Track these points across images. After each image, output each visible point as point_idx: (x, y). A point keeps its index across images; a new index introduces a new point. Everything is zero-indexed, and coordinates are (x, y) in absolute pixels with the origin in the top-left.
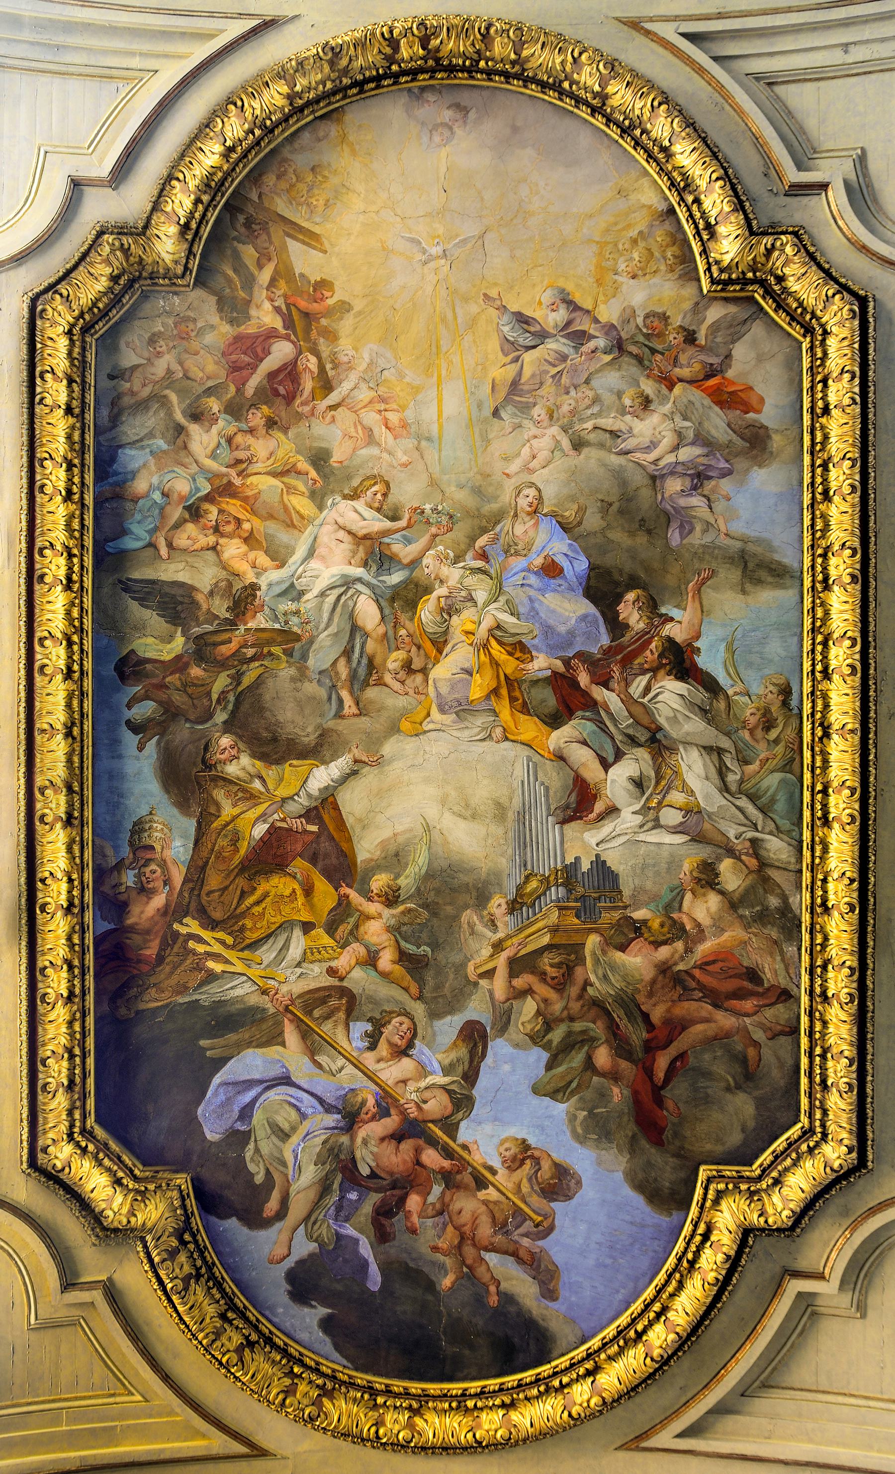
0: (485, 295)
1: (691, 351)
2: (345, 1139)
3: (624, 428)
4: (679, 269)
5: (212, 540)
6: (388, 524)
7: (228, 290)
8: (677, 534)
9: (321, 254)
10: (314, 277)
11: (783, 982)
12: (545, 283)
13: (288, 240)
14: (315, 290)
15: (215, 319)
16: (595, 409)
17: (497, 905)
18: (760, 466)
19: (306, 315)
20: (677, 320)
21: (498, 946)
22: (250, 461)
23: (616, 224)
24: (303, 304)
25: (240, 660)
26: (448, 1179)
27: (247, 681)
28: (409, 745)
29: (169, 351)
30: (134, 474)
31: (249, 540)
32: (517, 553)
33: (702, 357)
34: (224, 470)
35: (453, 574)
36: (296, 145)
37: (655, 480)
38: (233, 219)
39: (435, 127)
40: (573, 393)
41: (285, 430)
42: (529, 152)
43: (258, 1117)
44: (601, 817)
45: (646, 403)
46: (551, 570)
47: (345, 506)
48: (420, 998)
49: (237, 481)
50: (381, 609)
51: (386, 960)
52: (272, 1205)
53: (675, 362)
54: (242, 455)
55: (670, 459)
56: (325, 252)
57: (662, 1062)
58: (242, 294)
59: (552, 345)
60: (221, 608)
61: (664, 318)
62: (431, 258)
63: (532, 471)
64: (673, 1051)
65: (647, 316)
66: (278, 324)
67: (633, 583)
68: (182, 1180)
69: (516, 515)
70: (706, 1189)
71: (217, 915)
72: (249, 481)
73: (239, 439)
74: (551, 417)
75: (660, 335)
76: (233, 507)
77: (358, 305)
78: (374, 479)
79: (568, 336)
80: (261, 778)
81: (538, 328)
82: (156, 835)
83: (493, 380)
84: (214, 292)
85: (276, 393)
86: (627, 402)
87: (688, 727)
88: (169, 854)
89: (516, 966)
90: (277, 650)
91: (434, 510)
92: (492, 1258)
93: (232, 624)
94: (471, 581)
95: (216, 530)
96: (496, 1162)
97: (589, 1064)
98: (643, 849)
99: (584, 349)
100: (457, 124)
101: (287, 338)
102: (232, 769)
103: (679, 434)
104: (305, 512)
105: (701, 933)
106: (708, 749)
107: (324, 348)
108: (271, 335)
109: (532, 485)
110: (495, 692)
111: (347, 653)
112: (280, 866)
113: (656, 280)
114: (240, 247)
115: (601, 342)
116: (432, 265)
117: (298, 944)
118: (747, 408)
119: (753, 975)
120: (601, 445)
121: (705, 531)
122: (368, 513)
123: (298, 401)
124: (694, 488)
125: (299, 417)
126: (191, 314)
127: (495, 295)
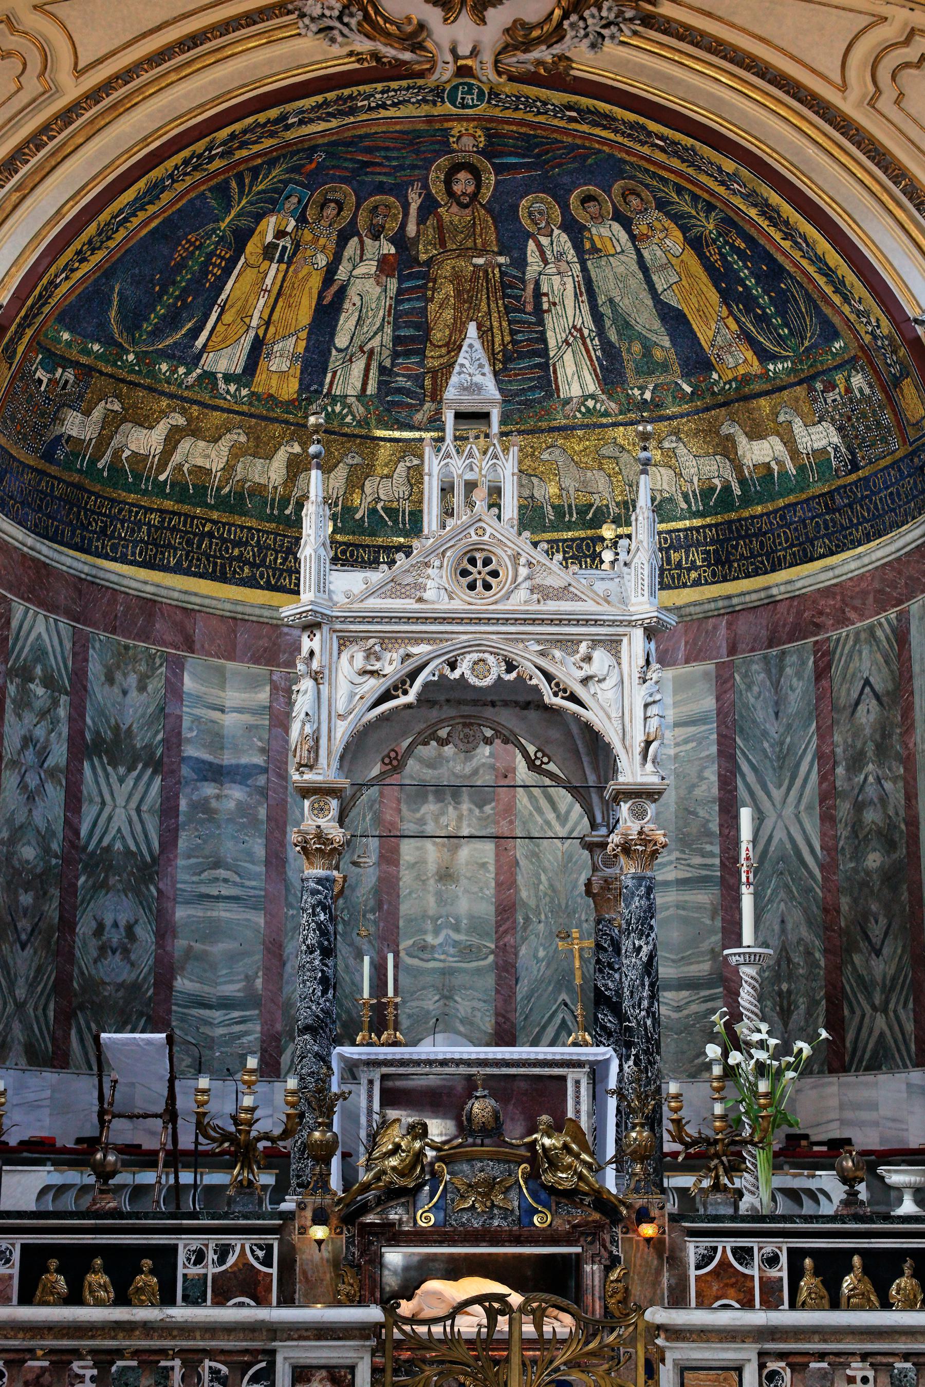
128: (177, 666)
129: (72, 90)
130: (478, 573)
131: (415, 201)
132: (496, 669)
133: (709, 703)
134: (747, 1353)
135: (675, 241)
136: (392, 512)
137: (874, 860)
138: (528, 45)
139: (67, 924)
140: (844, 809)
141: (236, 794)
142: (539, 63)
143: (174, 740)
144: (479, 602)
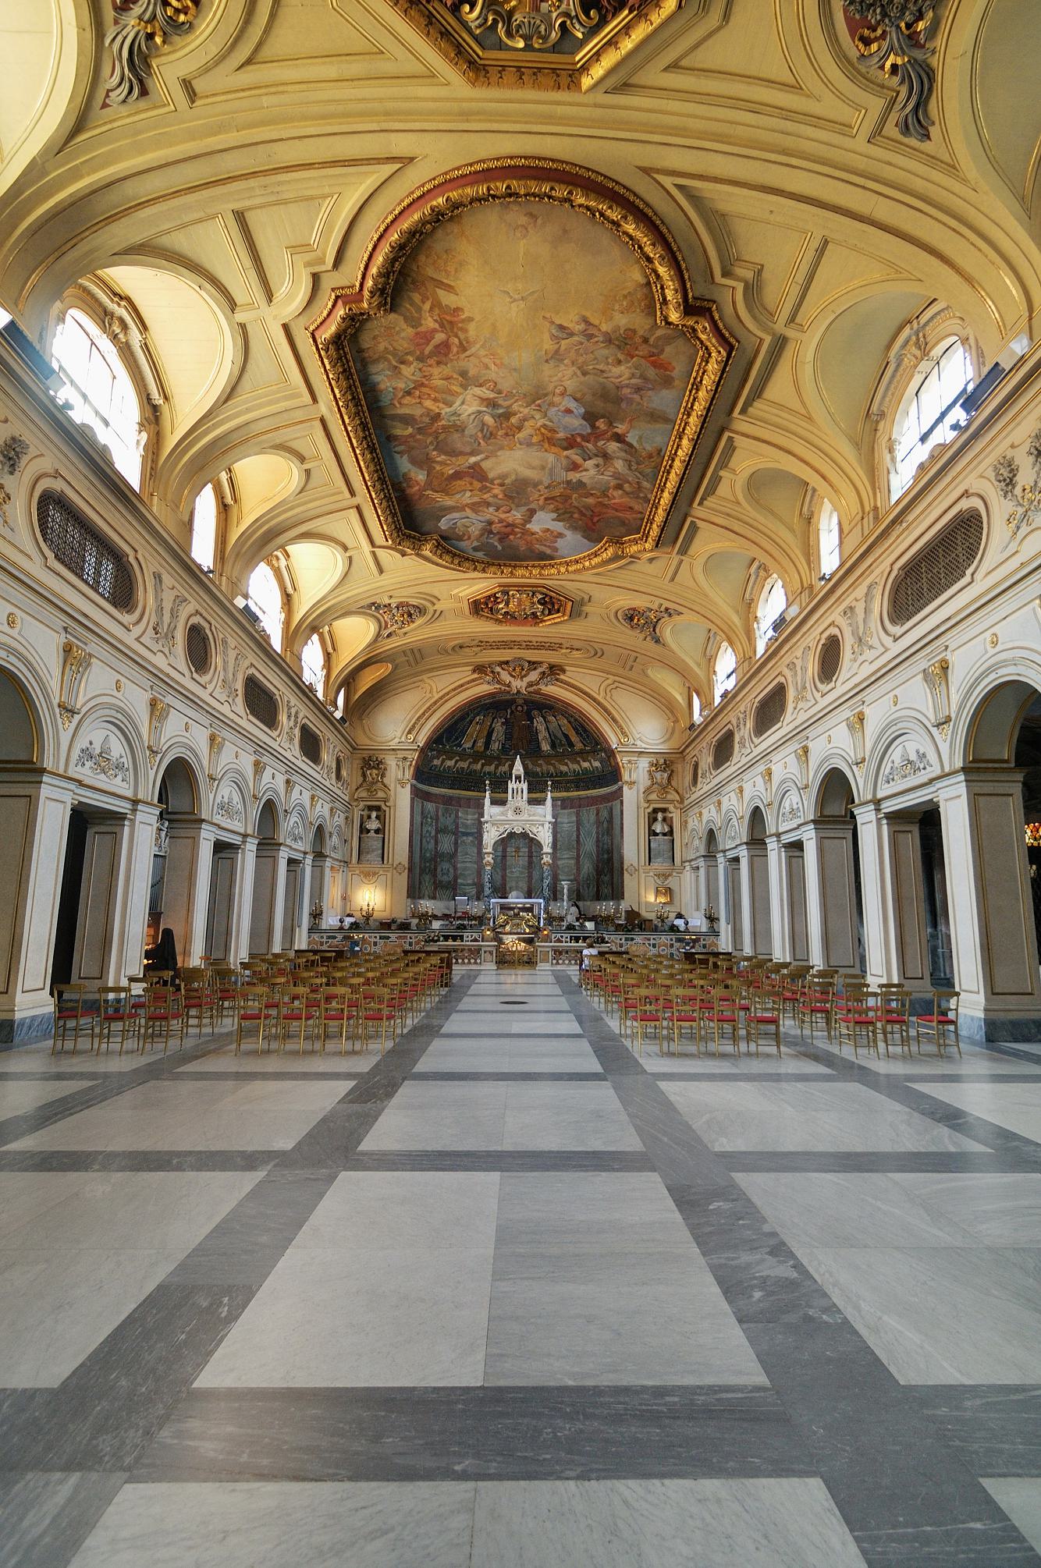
1: (644, 346)
4: (646, 311)
5: (418, 401)
10: (453, 306)
15: (405, 326)
16: (595, 362)
17: (539, 487)
19: (451, 323)
20: (641, 332)
22: (431, 375)
23: (617, 287)
24: (448, 318)
25: (436, 435)
26: (523, 533)
28: (508, 453)
30: (378, 383)
31: (435, 400)
35: (526, 411)
39: (517, 227)
41: (446, 365)
45: (619, 362)
46: (568, 411)
47: (476, 389)
49: (427, 382)
51: (500, 496)
52: (466, 537)
53: (637, 349)
54: (426, 374)
57: (596, 519)
59: (576, 338)
60: (427, 420)
61: (634, 331)
66: (437, 326)
67: (603, 417)
75: (631, 338)
76: (424, 390)
82: (413, 475)
86: (610, 360)
89: (546, 499)
93: (432, 424)
95: (419, 397)
97: (571, 516)
101: (442, 332)
102: (438, 459)
103: (633, 375)
105: (614, 498)
106: (626, 460)
107: (460, 334)
108: (434, 331)
111: (482, 430)
112: (461, 479)
113: (634, 315)
115: (601, 339)
117: (468, 494)
118: (666, 369)
120: (595, 374)
125: (452, 360)
128: (457, 813)
129: (437, 697)
130: (518, 811)
131: (509, 711)
132: (521, 830)
133: (575, 819)
134: (550, 949)
135: (565, 721)
136: (505, 773)
137: (606, 856)
138: (532, 686)
139: (436, 870)
140: (601, 844)
141: (471, 838)
143: (457, 827)
144: (518, 817)
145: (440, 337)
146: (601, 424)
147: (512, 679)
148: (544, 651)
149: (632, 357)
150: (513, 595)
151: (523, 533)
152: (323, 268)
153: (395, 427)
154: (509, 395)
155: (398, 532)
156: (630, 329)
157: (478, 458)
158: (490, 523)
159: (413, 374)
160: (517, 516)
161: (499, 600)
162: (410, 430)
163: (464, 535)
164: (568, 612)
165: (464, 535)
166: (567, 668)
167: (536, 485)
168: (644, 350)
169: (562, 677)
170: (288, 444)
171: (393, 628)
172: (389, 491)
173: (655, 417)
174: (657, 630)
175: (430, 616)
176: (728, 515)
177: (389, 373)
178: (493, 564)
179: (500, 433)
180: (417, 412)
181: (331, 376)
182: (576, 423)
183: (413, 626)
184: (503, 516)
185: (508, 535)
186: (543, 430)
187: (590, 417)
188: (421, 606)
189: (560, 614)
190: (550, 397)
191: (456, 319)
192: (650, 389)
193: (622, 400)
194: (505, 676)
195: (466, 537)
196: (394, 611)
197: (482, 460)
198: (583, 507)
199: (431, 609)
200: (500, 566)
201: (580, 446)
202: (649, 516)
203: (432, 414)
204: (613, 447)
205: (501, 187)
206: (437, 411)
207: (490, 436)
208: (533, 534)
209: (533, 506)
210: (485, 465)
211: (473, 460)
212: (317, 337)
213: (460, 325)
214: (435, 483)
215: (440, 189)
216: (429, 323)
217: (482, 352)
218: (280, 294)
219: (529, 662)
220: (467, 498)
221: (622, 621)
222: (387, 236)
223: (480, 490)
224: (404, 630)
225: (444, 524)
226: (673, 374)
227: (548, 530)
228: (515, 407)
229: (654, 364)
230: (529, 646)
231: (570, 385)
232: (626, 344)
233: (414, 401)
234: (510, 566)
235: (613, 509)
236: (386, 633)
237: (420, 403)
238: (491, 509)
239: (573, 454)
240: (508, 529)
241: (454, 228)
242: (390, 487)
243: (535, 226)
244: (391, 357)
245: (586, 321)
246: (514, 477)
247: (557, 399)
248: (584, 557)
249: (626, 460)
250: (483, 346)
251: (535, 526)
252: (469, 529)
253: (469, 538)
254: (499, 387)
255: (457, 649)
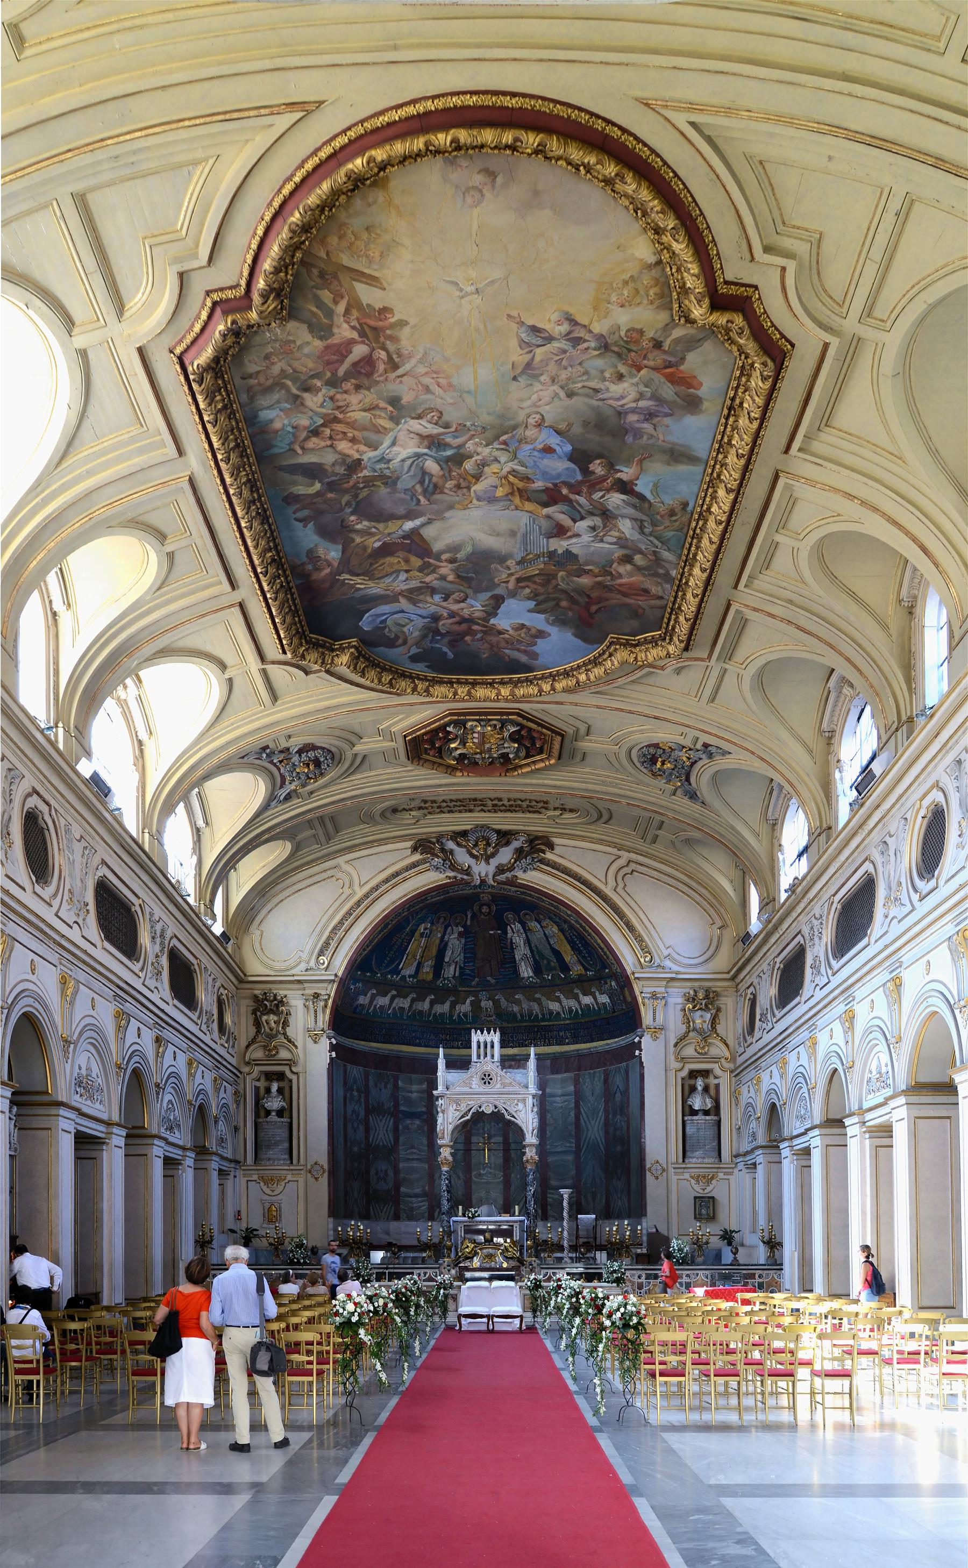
0: (509, 316)
1: (656, 353)
2: (433, 625)
3: (603, 387)
5: (329, 443)
6: (442, 430)
7: (314, 320)
8: (631, 439)
9: (381, 291)
11: (660, 594)
12: (555, 307)
13: (355, 283)
14: (379, 314)
15: (307, 337)
16: (585, 378)
17: (511, 563)
18: (692, 414)
19: (375, 329)
20: (650, 334)
21: (512, 574)
24: (372, 323)
25: (355, 490)
26: (485, 632)
27: (361, 497)
28: (460, 513)
29: (280, 360)
30: (272, 421)
31: (353, 440)
32: (526, 443)
33: (665, 357)
34: (330, 412)
35: (486, 451)
36: (351, 211)
37: (621, 414)
38: (309, 272)
40: (570, 369)
41: (368, 389)
42: (548, 212)
43: (389, 622)
44: (570, 537)
45: (620, 377)
46: (548, 450)
48: (469, 587)
49: (341, 416)
50: (440, 466)
51: (451, 578)
52: (400, 641)
53: (645, 358)
54: (341, 404)
55: (634, 405)
56: (384, 289)
57: (594, 608)
58: (325, 321)
59: (556, 344)
60: (341, 470)
61: (641, 332)
62: (467, 294)
63: (539, 407)
64: (600, 605)
65: (628, 331)
66: (355, 335)
67: (599, 456)
68: (354, 642)
69: (526, 426)
70: (611, 643)
71: (359, 572)
72: (348, 415)
73: (338, 396)
74: (553, 381)
75: (637, 342)
76: (339, 427)
77: (413, 321)
78: (432, 410)
79: (568, 340)
80: (375, 527)
81: (547, 335)
82: (321, 552)
83: (513, 363)
84: (303, 321)
85: (360, 373)
86: (607, 375)
87: (624, 511)
88: (329, 557)
89: (519, 580)
90: (378, 483)
91: (473, 425)
92: (506, 651)
93: (349, 476)
94: (497, 453)
95: (331, 438)
96: (509, 629)
97: (558, 605)
98: (592, 549)
99: (580, 347)
100: (486, 187)
101: (363, 342)
102: (359, 527)
104: (387, 426)
105: (620, 576)
106: (636, 520)
107: (391, 346)
108: (351, 342)
109: (538, 413)
110: (512, 494)
111: (421, 482)
112: (392, 554)
114: (319, 292)
115: (593, 344)
116: (467, 299)
117: (403, 576)
118: (690, 386)
119: (646, 591)
120: (587, 395)
121: (648, 439)
122: (429, 425)
123: (376, 375)
124: (647, 420)
125: (378, 383)
126: (291, 338)
127: (516, 315)
142: (507, 878)
145: (360, 350)
146: (597, 468)
147: (472, 862)
148: (520, 815)
149: (639, 369)
150: (472, 728)
151: (485, 632)
152: (196, 264)
153: (295, 483)
154: (461, 428)
155: (301, 639)
156: (633, 329)
157: (417, 522)
158: (436, 618)
159: (322, 406)
160: (475, 606)
161: (451, 736)
162: (318, 486)
163: (397, 637)
164: (556, 752)
165: (397, 637)
166: (556, 841)
167: (502, 559)
168: (656, 359)
169: (549, 856)
170: (141, 518)
171: (293, 787)
172: (286, 577)
173: (677, 455)
174: (693, 779)
175: (347, 765)
176: (790, 602)
177: (288, 406)
178: (441, 682)
179: (449, 484)
180: (328, 459)
181: (206, 418)
182: (560, 466)
183: (321, 781)
184: (455, 607)
185: (462, 635)
186: (511, 478)
187: (580, 458)
188: (333, 749)
189: (544, 756)
190: (520, 431)
191: (381, 323)
192: (667, 415)
193: (627, 432)
194: (462, 857)
195: (400, 641)
196: (296, 759)
197: (423, 525)
198: (575, 590)
199: (349, 754)
200: (451, 683)
201: (566, 500)
202: (674, 603)
203: (349, 460)
204: (616, 499)
205: (442, 139)
206: (357, 456)
207: (433, 489)
208: (500, 633)
209: (499, 591)
210: (428, 533)
211: (409, 525)
212: (187, 362)
213: (388, 332)
214: (355, 561)
215: (357, 145)
216: (344, 331)
217: (421, 369)
218: (135, 302)
219: (498, 832)
220: (401, 583)
221: (638, 765)
222: (285, 213)
223: (420, 570)
224: (309, 788)
225: (366, 623)
226: (699, 393)
227: (523, 626)
228: (470, 446)
229: (672, 379)
230: (497, 806)
231: (551, 412)
232: (630, 350)
233: (323, 444)
234: (466, 683)
235: (620, 592)
236: (283, 793)
237: (331, 446)
238: (437, 598)
239: (557, 512)
240: (464, 626)
241: (379, 196)
242: (288, 572)
243: (493, 187)
244: (289, 383)
245: (573, 322)
246: (469, 549)
247: (531, 433)
248: (579, 667)
249: (636, 520)
250: (421, 361)
251: (502, 622)
252: (405, 629)
253: (405, 642)
254: (446, 417)
255: (388, 814)
